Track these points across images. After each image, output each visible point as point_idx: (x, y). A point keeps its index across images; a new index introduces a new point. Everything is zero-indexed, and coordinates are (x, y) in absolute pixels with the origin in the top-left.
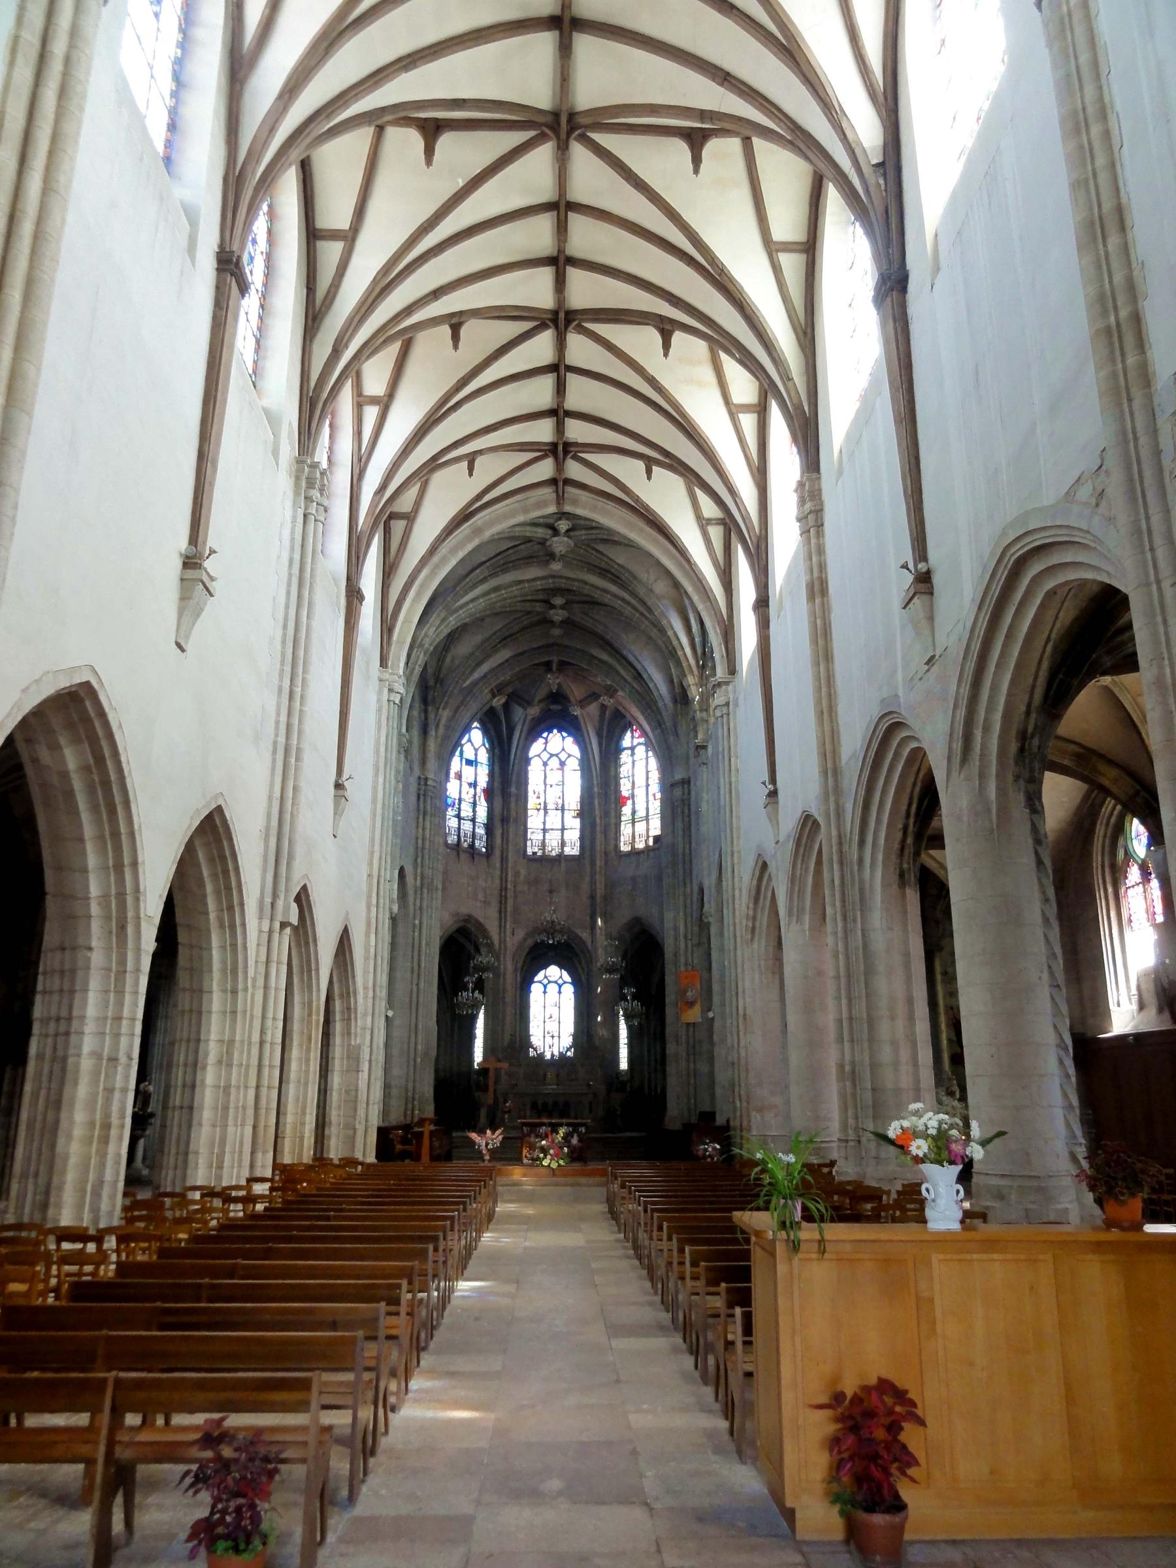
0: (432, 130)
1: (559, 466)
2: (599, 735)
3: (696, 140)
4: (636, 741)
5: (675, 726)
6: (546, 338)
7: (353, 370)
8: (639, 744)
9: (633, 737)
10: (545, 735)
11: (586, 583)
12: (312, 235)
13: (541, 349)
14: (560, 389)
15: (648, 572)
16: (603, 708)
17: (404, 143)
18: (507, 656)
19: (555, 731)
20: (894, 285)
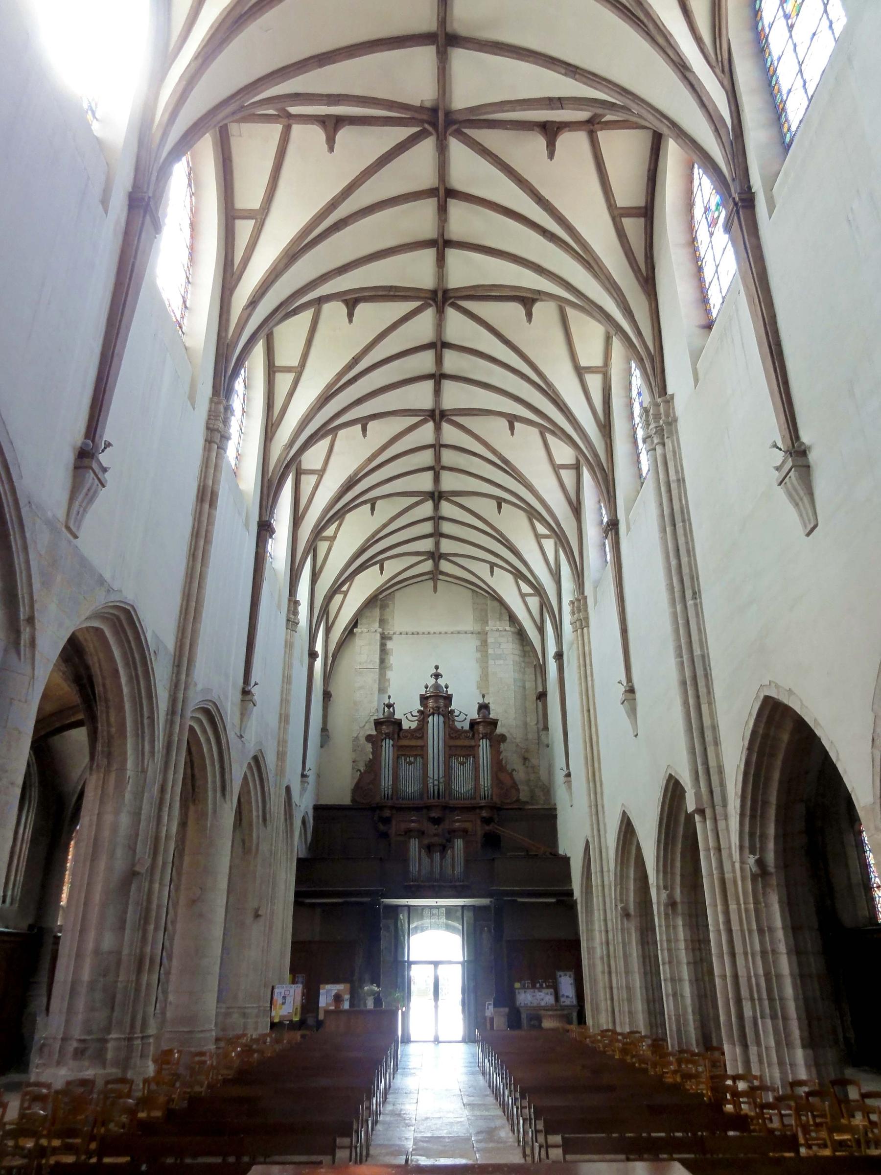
0: (332, 125)
1: (438, 429)
3: (551, 131)
6: (429, 315)
7: (266, 331)
12: (230, 215)
13: (422, 327)
14: (439, 360)
17: (307, 138)
20: (743, 207)
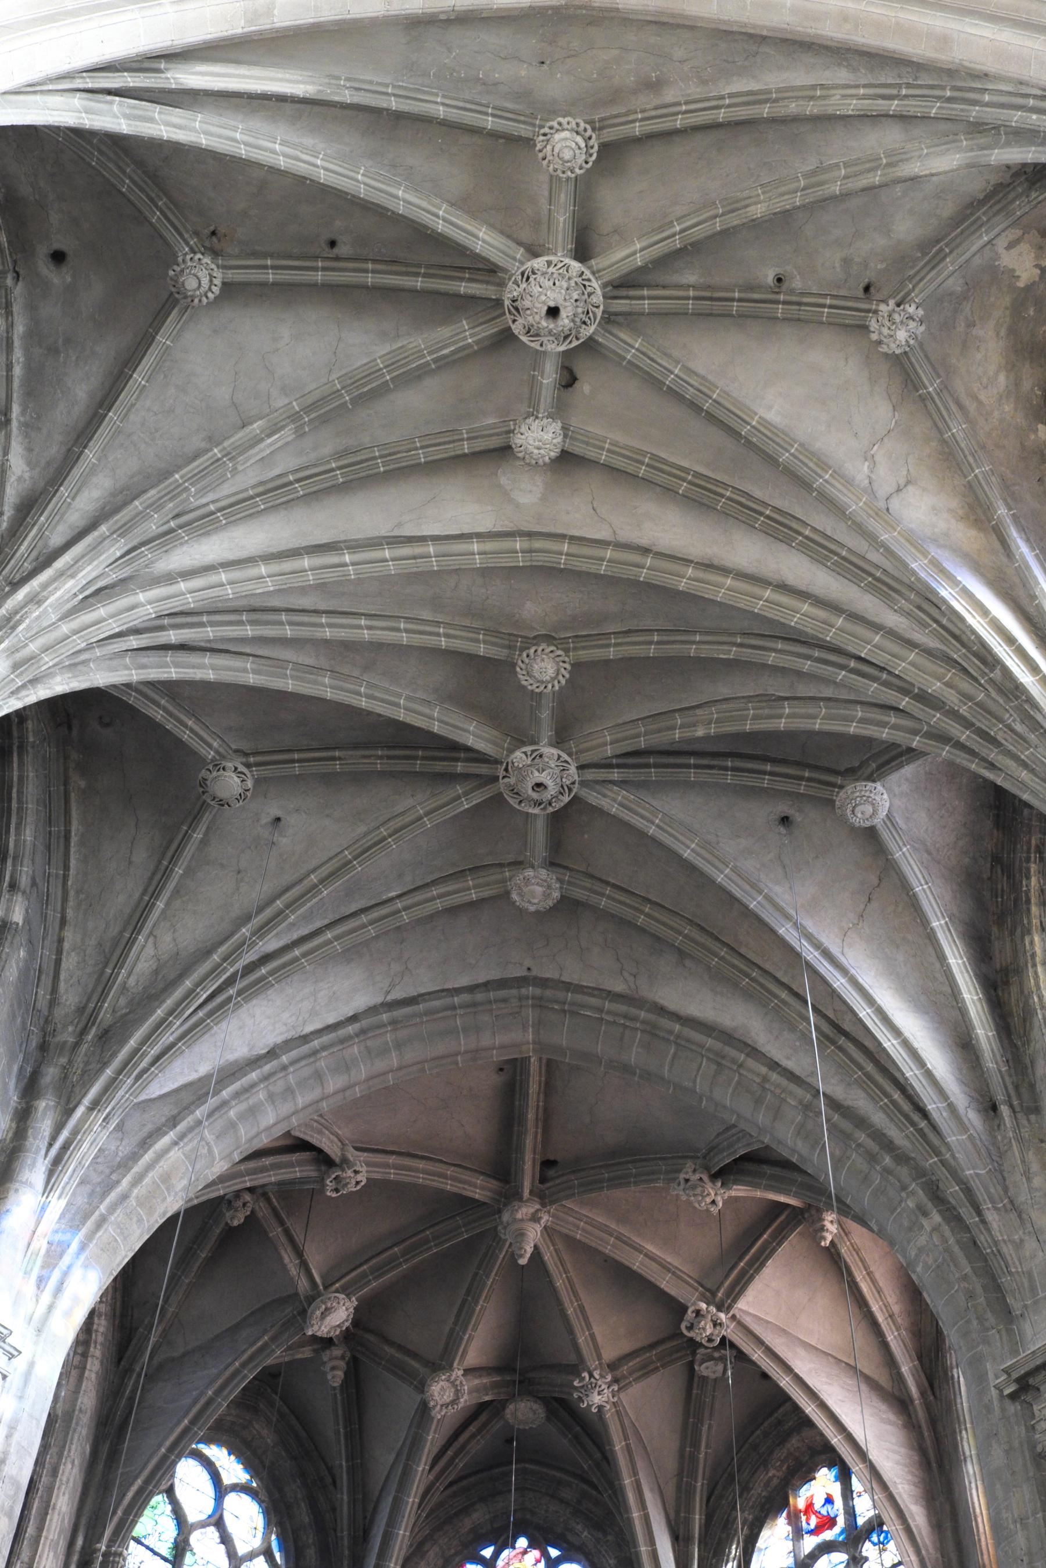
2: (679, 1539)
4: (809, 1543)
5: (1000, 1174)
8: (826, 1548)
9: (798, 1534)
10: (487, 1553)
11: (645, 551)
15: (868, 457)
16: (694, 1394)
18: (361, 1002)
19: (522, 1542)
